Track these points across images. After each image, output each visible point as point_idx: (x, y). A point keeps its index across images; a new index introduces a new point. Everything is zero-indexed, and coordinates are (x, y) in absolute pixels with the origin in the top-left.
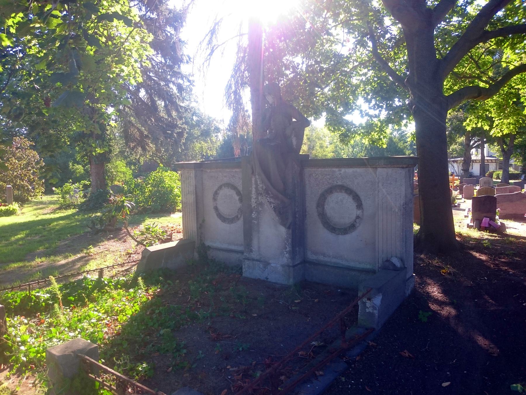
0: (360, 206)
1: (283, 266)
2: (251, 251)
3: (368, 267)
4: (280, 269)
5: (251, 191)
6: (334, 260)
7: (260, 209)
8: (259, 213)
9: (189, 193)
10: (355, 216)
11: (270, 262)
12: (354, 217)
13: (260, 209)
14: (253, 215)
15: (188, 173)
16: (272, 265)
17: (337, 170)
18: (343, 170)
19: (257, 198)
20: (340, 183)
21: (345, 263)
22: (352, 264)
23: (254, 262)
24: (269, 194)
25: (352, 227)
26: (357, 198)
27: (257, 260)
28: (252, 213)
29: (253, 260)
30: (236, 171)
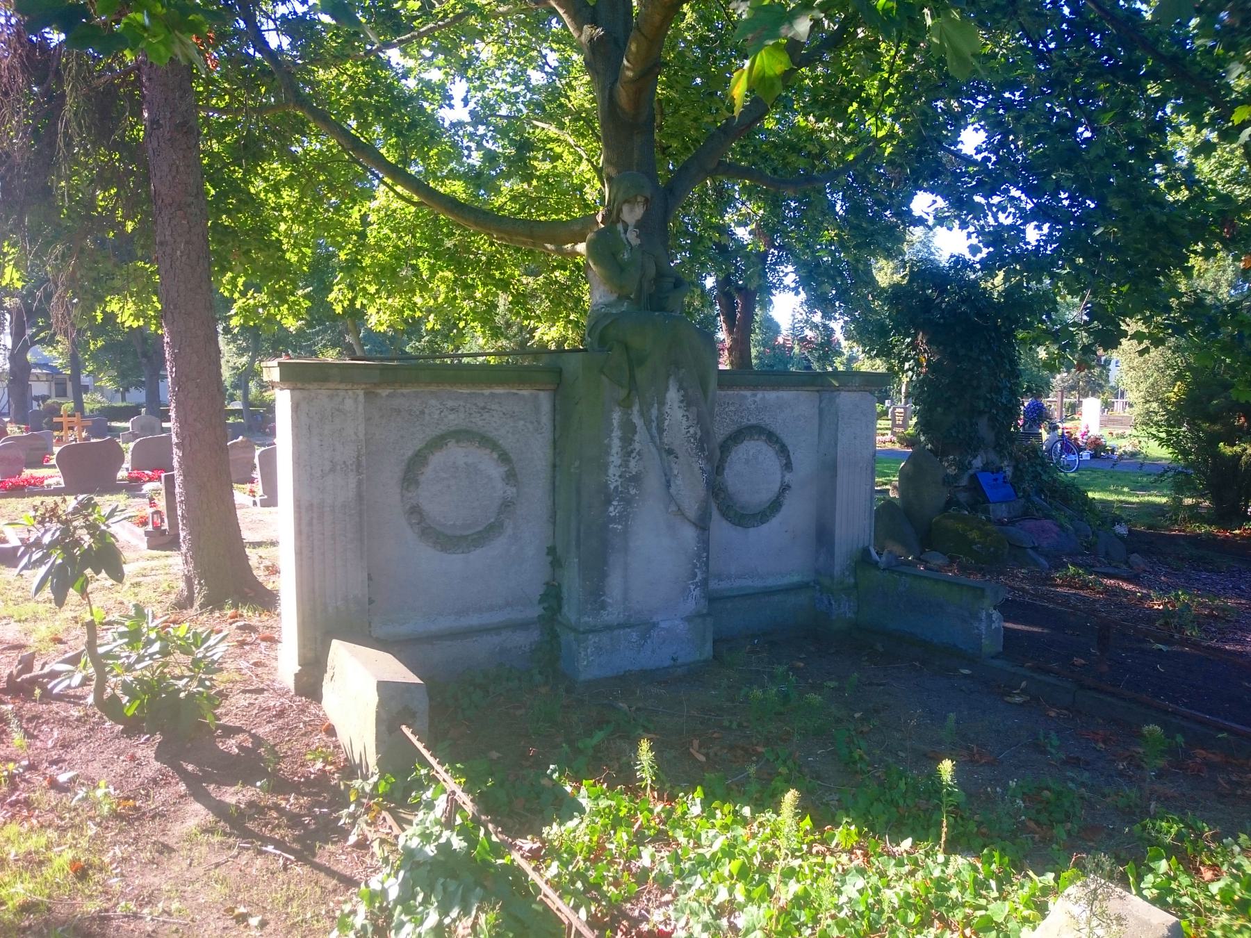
0: (788, 466)
1: (688, 619)
2: (603, 606)
3: (796, 579)
4: (681, 627)
5: (609, 446)
6: (738, 583)
7: (633, 492)
8: (628, 501)
9: (333, 470)
10: (778, 485)
11: (655, 619)
12: (776, 487)
14: (611, 509)
15: (331, 397)
16: (662, 625)
17: (748, 393)
18: (760, 394)
19: (625, 464)
20: (753, 422)
21: (758, 583)
22: (771, 582)
23: (616, 632)
24: (702, 450)
25: (775, 505)
26: (783, 450)
27: (621, 626)
28: (609, 502)
29: (609, 628)
30: (492, 395)
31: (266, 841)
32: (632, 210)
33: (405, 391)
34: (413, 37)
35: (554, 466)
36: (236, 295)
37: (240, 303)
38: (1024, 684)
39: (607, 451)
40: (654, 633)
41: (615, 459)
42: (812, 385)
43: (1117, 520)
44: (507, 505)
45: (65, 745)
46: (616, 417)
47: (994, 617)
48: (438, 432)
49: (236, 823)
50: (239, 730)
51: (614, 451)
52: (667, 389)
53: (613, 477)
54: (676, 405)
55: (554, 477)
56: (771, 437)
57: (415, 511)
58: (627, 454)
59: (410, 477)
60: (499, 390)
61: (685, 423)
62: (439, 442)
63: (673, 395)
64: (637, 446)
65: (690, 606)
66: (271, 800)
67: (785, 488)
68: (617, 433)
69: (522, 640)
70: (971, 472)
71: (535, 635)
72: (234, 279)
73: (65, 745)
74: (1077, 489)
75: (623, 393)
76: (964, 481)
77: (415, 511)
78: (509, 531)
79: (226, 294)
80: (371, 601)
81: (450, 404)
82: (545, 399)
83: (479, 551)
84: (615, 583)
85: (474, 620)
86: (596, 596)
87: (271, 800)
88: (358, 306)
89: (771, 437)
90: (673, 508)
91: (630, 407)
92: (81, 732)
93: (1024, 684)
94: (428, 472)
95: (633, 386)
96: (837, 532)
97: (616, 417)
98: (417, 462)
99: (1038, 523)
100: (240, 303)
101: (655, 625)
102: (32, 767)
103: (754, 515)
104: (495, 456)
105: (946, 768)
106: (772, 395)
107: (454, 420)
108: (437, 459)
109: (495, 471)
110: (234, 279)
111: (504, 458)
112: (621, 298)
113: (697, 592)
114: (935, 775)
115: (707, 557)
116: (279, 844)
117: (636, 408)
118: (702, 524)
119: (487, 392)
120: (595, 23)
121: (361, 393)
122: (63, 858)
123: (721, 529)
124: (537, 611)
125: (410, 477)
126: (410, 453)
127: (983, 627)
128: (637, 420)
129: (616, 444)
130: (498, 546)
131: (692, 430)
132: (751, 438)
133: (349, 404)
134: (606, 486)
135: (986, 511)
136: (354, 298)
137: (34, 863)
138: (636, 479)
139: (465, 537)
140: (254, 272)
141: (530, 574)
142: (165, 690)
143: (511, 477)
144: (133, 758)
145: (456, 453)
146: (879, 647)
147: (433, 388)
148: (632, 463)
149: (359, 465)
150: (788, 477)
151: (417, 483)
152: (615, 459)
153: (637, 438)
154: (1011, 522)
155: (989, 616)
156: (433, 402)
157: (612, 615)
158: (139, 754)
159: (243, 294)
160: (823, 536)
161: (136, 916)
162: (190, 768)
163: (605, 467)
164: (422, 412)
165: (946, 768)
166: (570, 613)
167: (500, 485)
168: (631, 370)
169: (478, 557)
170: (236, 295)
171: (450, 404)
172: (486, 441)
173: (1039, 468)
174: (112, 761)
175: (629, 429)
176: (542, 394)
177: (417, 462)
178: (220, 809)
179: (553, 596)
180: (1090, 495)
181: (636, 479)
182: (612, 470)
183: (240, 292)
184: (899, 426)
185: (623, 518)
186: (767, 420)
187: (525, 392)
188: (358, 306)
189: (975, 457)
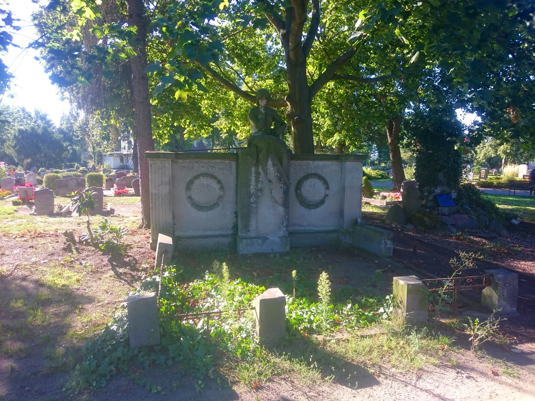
0: (327, 188)
1: (280, 238)
2: (249, 231)
3: (331, 228)
4: (278, 240)
5: (251, 179)
6: (307, 228)
7: (260, 194)
8: (258, 197)
9: (162, 184)
11: (268, 237)
13: (260, 194)
15: (161, 163)
16: (271, 239)
17: (311, 162)
18: (316, 162)
19: (257, 185)
20: (313, 172)
21: (316, 229)
22: (320, 229)
24: (281, 180)
25: (322, 202)
26: (325, 182)
27: (255, 238)
28: (251, 198)
30: (216, 162)
31: (123, 279)
32: (262, 101)
33: (187, 161)
34: (237, 33)
35: (237, 185)
36: (186, 126)
37: (188, 129)
38: (389, 266)
39: (250, 180)
40: (267, 241)
41: (253, 183)
42: (337, 159)
43: (516, 217)
44: (220, 197)
45: (87, 256)
46: (253, 169)
47: (388, 243)
48: (197, 174)
49: (119, 276)
50: (131, 256)
51: (252, 181)
52: (268, 161)
53: (252, 189)
54: (271, 166)
55: (237, 189)
56: (320, 177)
57: (190, 198)
58: (257, 181)
59: (188, 188)
60: (218, 161)
61: (274, 172)
62: (197, 177)
63: (270, 163)
64: (261, 179)
65: (282, 233)
66: (130, 272)
67: (326, 195)
68: (253, 175)
69: (226, 241)
70: (434, 194)
71: (230, 239)
72: (185, 121)
73: (87, 256)
74: (491, 203)
75: (255, 162)
76: (431, 198)
77: (190, 198)
78: (221, 206)
79: (183, 126)
80: (174, 224)
81: (202, 165)
82: (233, 164)
83: (211, 212)
84: (253, 224)
85: (210, 233)
86: (246, 227)
87: (130, 272)
88: (232, 129)
89: (320, 177)
90: (274, 200)
91: (258, 166)
92: (93, 253)
93: (389, 266)
94: (194, 186)
95: (258, 160)
96: (345, 211)
97: (253, 169)
98: (191, 182)
99: (461, 215)
100: (188, 129)
101: (267, 239)
102: (77, 260)
103: (313, 205)
104: (216, 181)
105: (294, 272)
106: (321, 163)
107: (203, 170)
108: (197, 182)
109: (217, 186)
110: (185, 121)
111: (219, 182)
112: (259, 131)
113: (284, 229)
114: (291, 274)
115: (288, 218)
116: (125, 281)
117: (260, 167)
118: (286, 205)
119: (214, 161)
120: (284, 29)
121: (170, 161)
122: (74, 278)
123: (298, 210)
124: (231, 232)
125: (188, 188)
126: (188, 180)
127: (383, 246)
128: (260, 170)
129: (253, 179)
130: (217, 210)
131: (276, 174)
132: (312, 178)
133: (167, 165)
134: (250, 192)
135: (438, 210)
136: (231, 127)
137: (69, 278)
138: (261, 190)
139: (206, 207)
140: (192, 118)
141: (228, 220)
142: (112, 243)
143: (222, 188)
144: (102, 260)
145: (204, 181)
146: (356, 253)
147: (195, 160)
148: (259, 185)
149: (170, 183)
150: (327, 192)
151: (190, 189)
152: (253, 183)
153: (261, 176)
154: (449, 215)
155: (386, 243)
156: (196, 164)
157: (252, 234)
158: (104, 259)
159: (189, 126)
160: (341, 213)
161: (85, 290)
162: (114, 263)
163: (249, 186)
164: (192, 168)
165: (294, 272)
166: (240, 234)
167: (218, 191)
168: (257, 154)
169: (211, 213)
170: (186, 126)
171: (202, 165)
172: (213, 177)
173: (471, 194)
174: (97, 260)
175: (258, 174)
176: (232, 162)
177: (191, 182)
178: (116, 273)
179: (235, 227)
180: (498, 206)
181: (261, 190)
182: (252, 187)
183: (188, 125)
184: (483, 178)
185: (256, 202)
186: (319, 171)
187: (227, 162)
188: (232, 129)
189: (436, 188)
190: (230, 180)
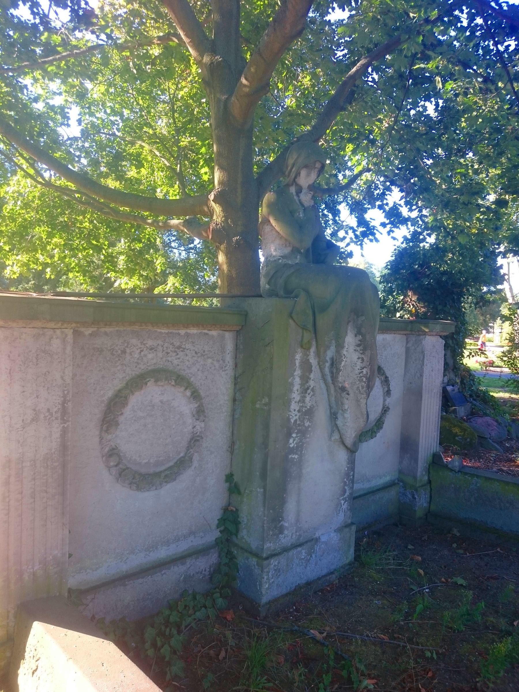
0: (388, 393)
1: (339, 530)
3: (387, 479)
5: (292, 384)
8: (303, 433)
10: (381, 407)
11: (317, 535)
12: (379, 409)
13: (307, 424)
14: (291, 441)
19: (302, 400)
23: (291, 553)
27: (295, 546)
28: (289, 435)
29: (286, 550)
30: (187, 335)
32: (308, 175)
33: (108, 330)
35: (234, 400)
41: (296, 396)
44: (195, 440)
51: (295, 389)
54: (351, 349)
55: (234, 411)
57: (112, 453)
58: (304, 390)
59: (109, 419)
60: (194, 331)
62: (138, 382)
64: (312, 383)
68: (298, 372)
69: (203, 564)
78: (195, 464)
81: (150, 343)
82: (229, 338)
83: (169, 486)
84: (291, 507)
86: (276, 520)
91: (309, 349)
101: (317, 540)
104: (188, 393)
107: (153, 360)
108: (136, 399)
111: (196, 396)
112: (295, 251)
117: (313, 349)
119: (182, 332)
120: (213, 51)
121: (69, 332)
125: (109, 419)
126: (110, 394)
128: (313, 361)
129: (297, 381)
133: (56, 343)
134: (289, 420)
139: (157, 474)
143: (200, 413)
145: (153, 393)
148: (308, 399)
152: (296, 396)
153: (312, 376)
156: (134, 341)
163: (287, 403)
164: (124, 352)
167: (189, 420)
169: (168, 492)
171: (150, 343)
172: (181, 380)
175: (307, 367)
185: (299, 448)
187: (214, 333)
190: (219, 385)
